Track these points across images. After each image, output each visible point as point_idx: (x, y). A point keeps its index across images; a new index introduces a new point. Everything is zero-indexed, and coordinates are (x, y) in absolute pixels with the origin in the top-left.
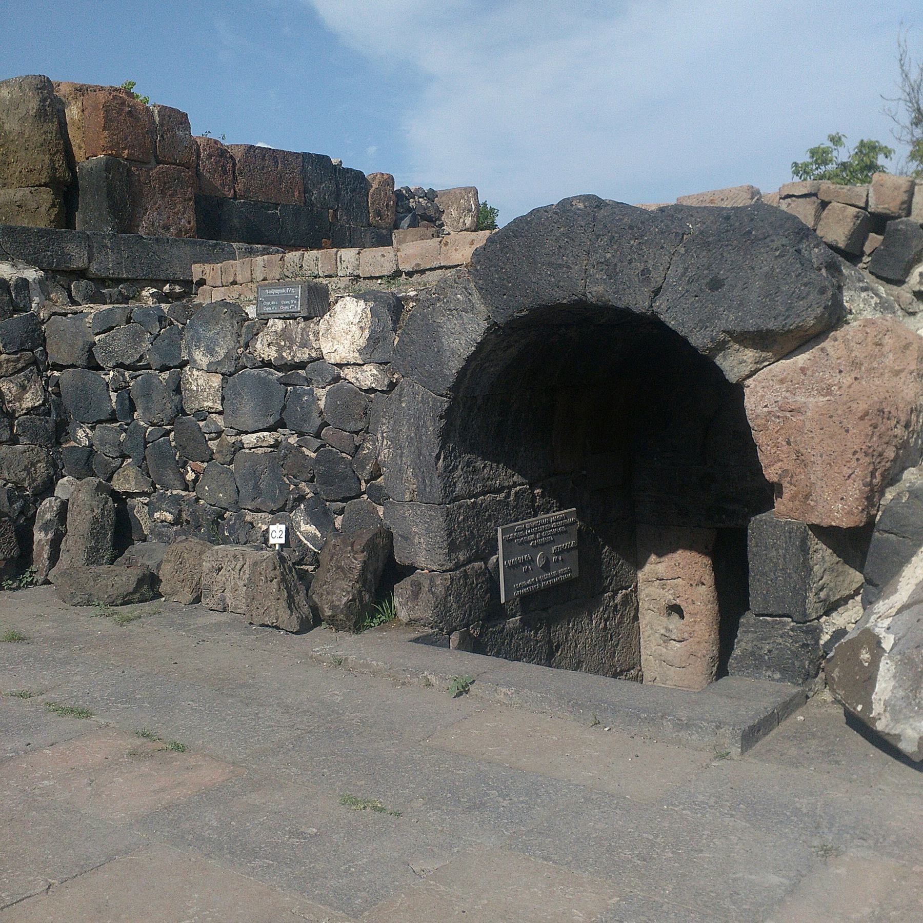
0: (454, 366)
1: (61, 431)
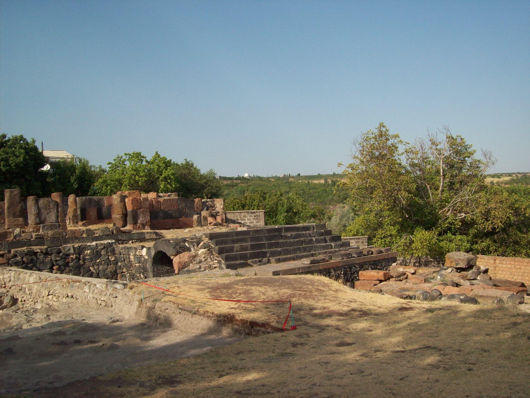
0: (152, 257)
1: (117, 263)
